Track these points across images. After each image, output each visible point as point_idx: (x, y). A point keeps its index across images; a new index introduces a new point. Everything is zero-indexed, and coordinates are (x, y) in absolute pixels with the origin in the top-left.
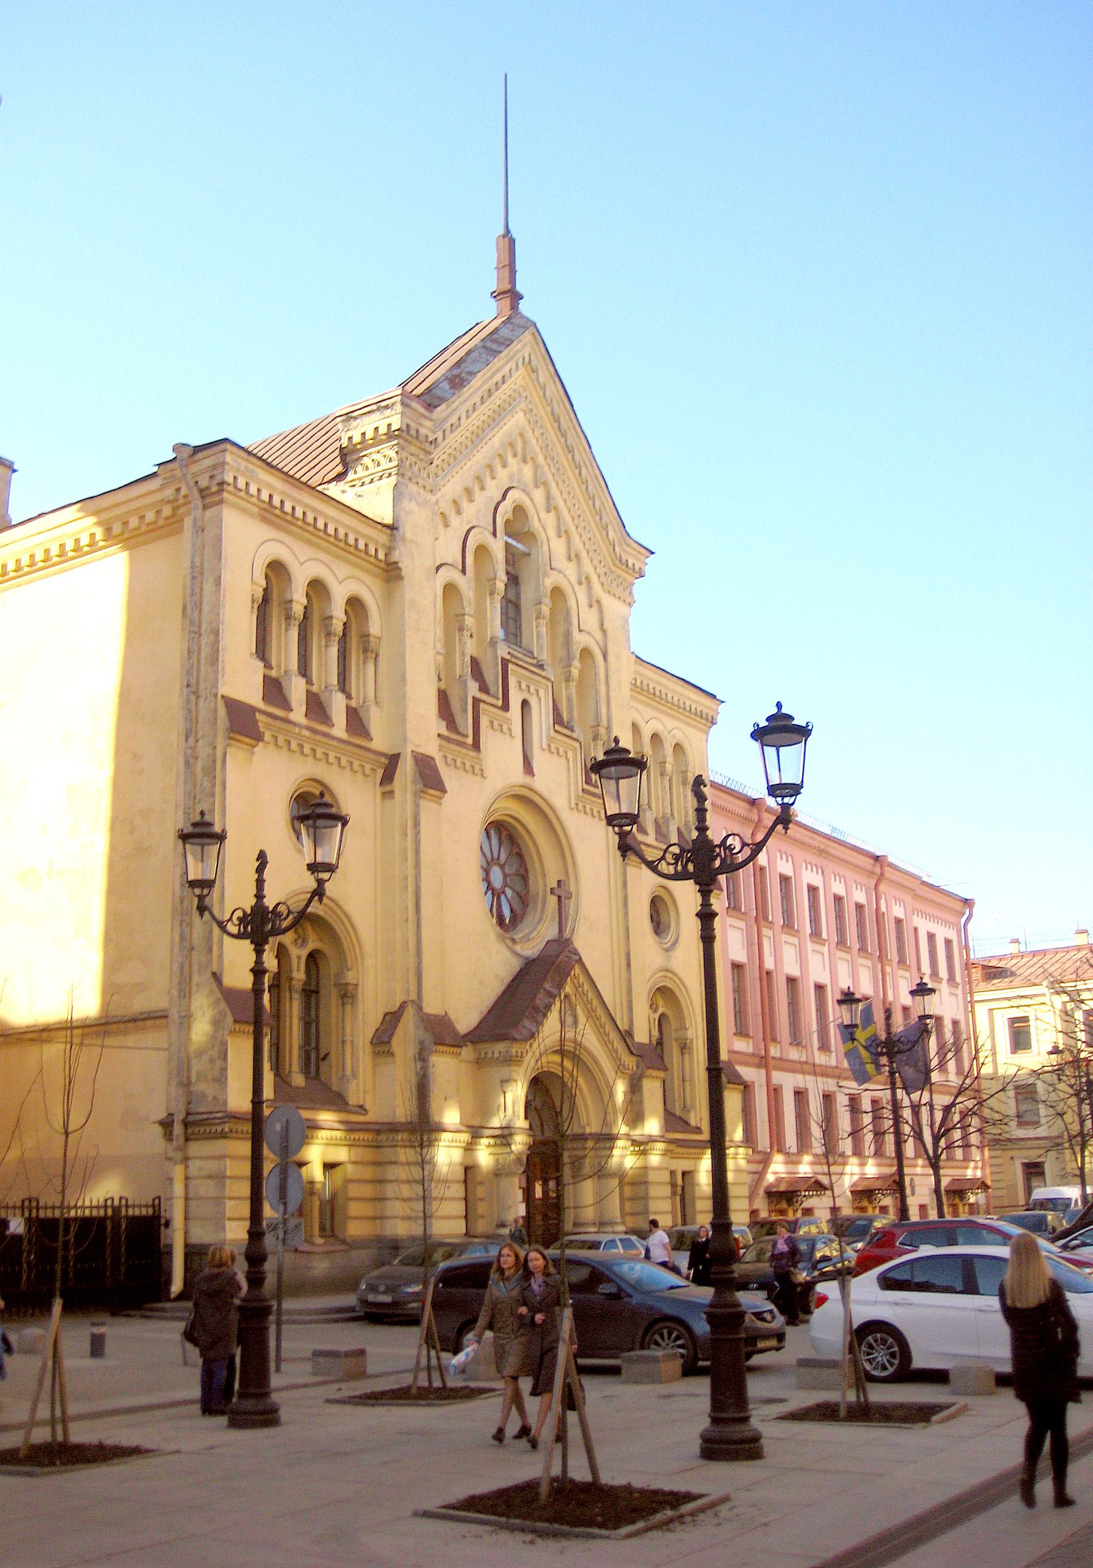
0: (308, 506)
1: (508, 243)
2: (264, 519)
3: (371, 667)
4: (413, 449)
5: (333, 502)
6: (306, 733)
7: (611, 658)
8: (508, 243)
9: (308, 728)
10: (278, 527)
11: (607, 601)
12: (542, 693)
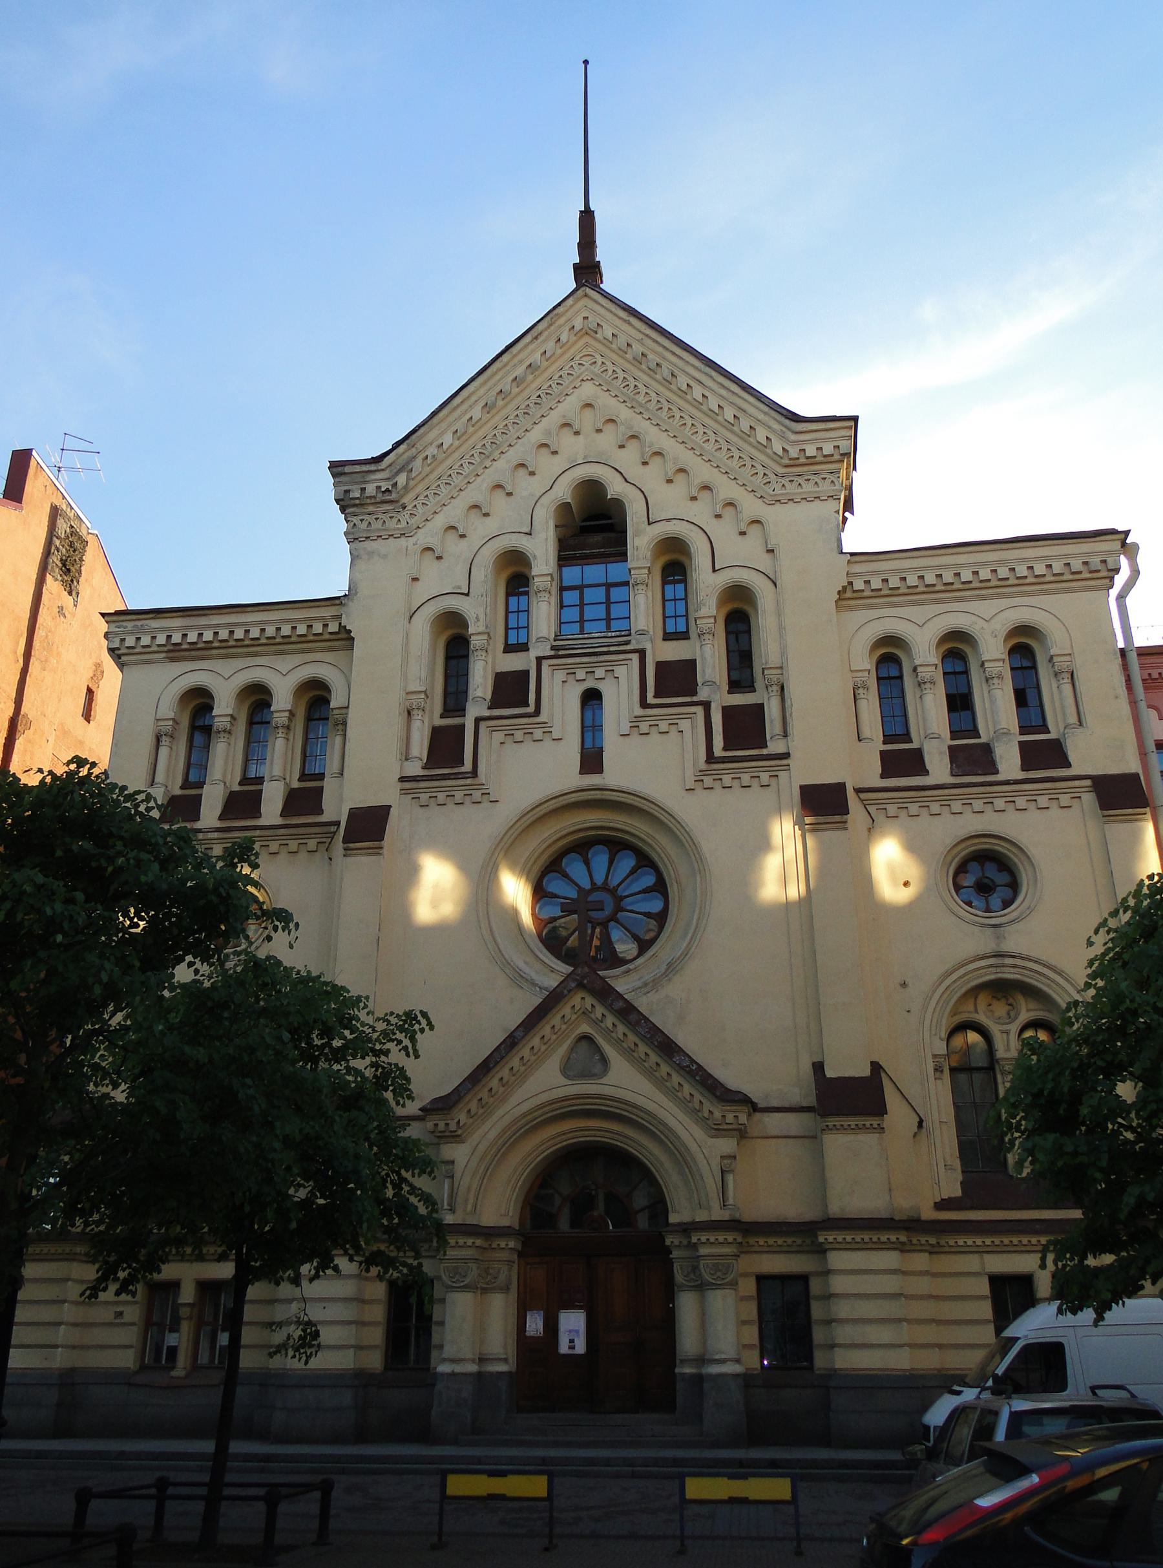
0: (218, 625)
1: (587, 219)
2: (173, 660)
3: (338, 740)
4: (371, 509)
5: (249, 609)
6: (215, 835)
7: (786, 578)
8: (587, 219)
9: (218, 830)
10: (193, 659)
11: (771, 514)
12: (620, 671)
